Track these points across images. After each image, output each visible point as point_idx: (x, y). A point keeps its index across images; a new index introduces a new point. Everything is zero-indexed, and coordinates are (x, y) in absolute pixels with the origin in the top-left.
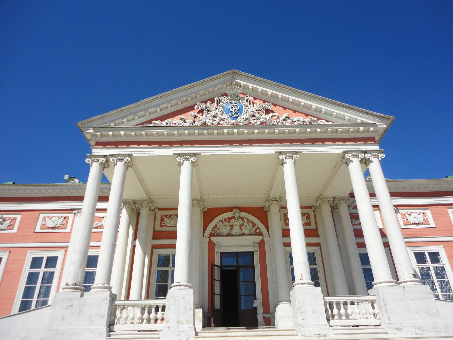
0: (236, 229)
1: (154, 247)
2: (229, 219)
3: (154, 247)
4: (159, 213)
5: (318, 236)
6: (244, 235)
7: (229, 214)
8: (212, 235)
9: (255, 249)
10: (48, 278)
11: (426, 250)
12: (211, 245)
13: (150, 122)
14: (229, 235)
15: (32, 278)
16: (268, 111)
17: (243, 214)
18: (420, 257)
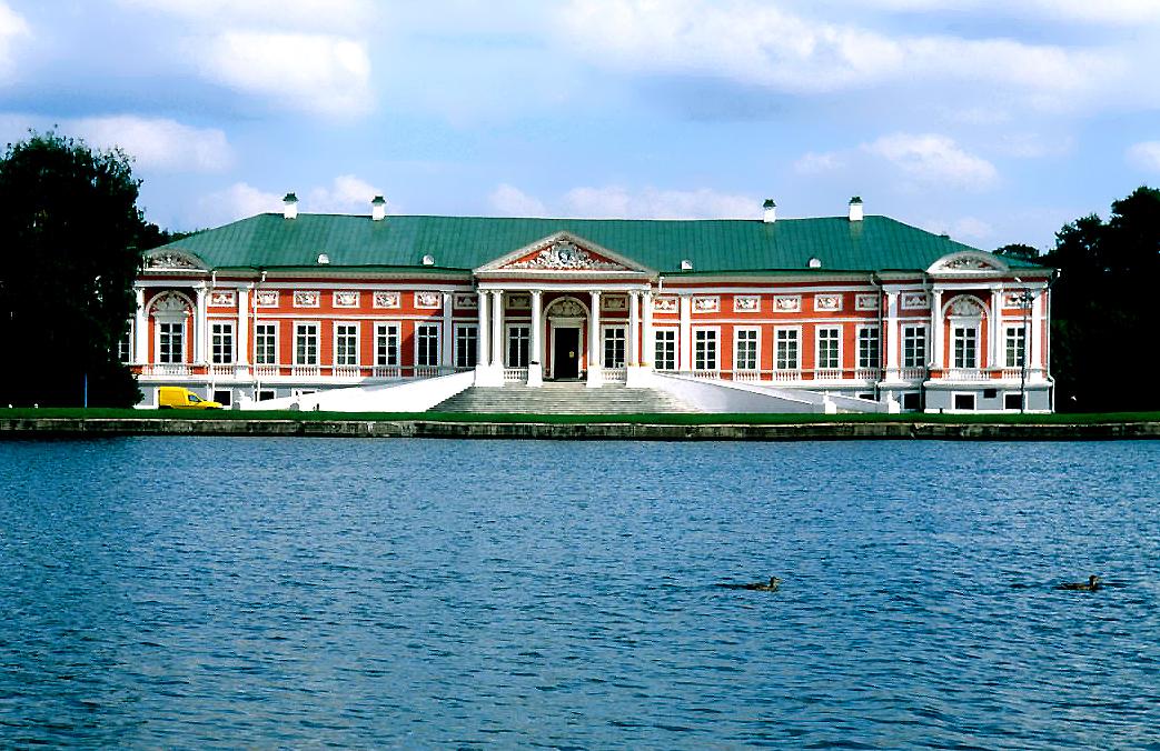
0: (567, 312)
1: (507, 322)
2: (562, 302)
3: (507, 322)
4: (509, 295)
5: (628, 317)
6: (572, 316)
7: (562, 299)
8: (548, 315)
9: (581, 327)
10: (434, 342)
11: (706, 329)
12: (548, 322)
13: (512, 263)
14: (562, 316)
15: (423, 342)
16: (586, 258)
17: (574, 299)
18: (701, 335)
